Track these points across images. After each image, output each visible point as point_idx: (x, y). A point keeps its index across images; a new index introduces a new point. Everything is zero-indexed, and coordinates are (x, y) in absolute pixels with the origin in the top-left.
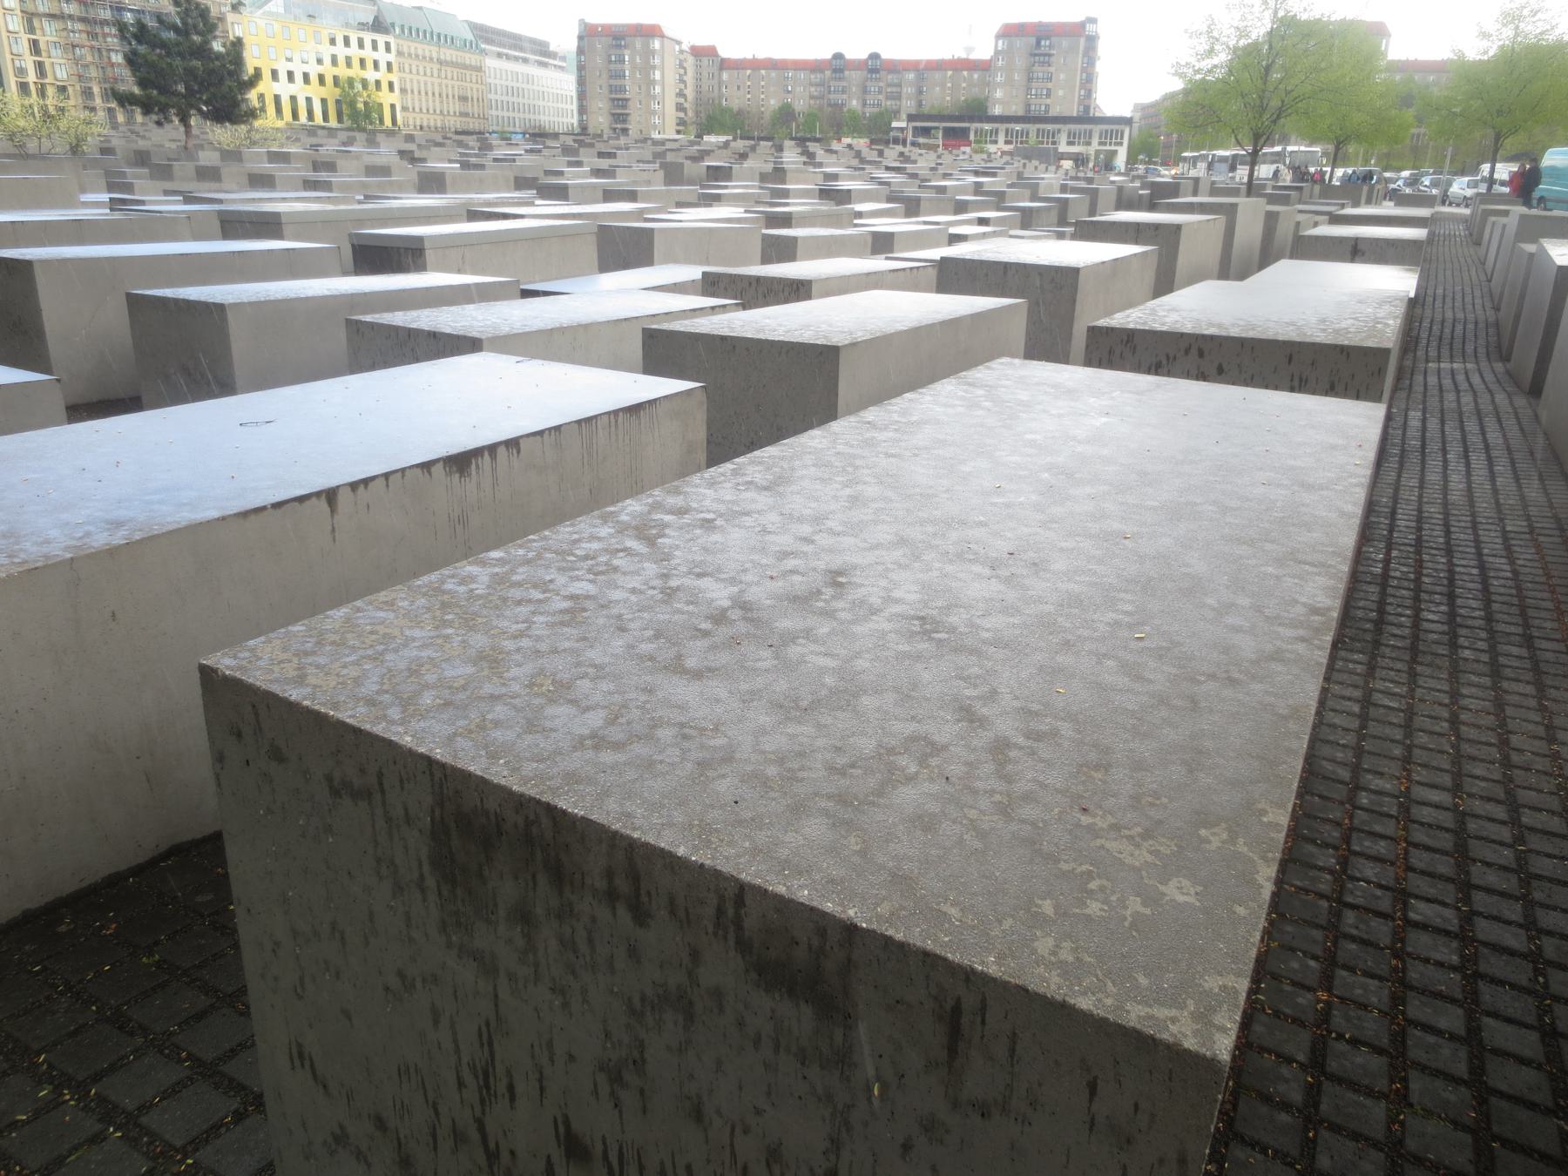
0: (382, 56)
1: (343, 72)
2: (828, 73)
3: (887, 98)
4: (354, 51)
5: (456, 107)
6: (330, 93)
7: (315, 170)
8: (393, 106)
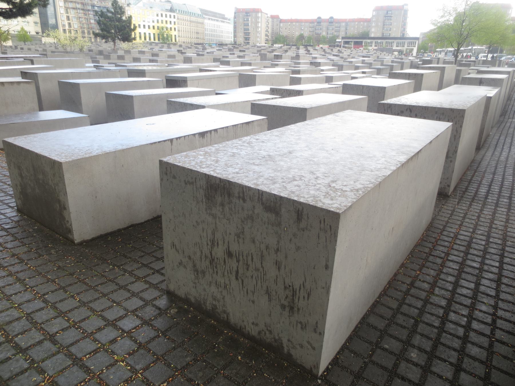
0: (173, 20)
1: (160, 25)
2: (316, 23)
3: (335, 32)
4: (164, 19)
5: (195, 35)
6: (156, 31)
7: (168, 58)
8: (175, 36)
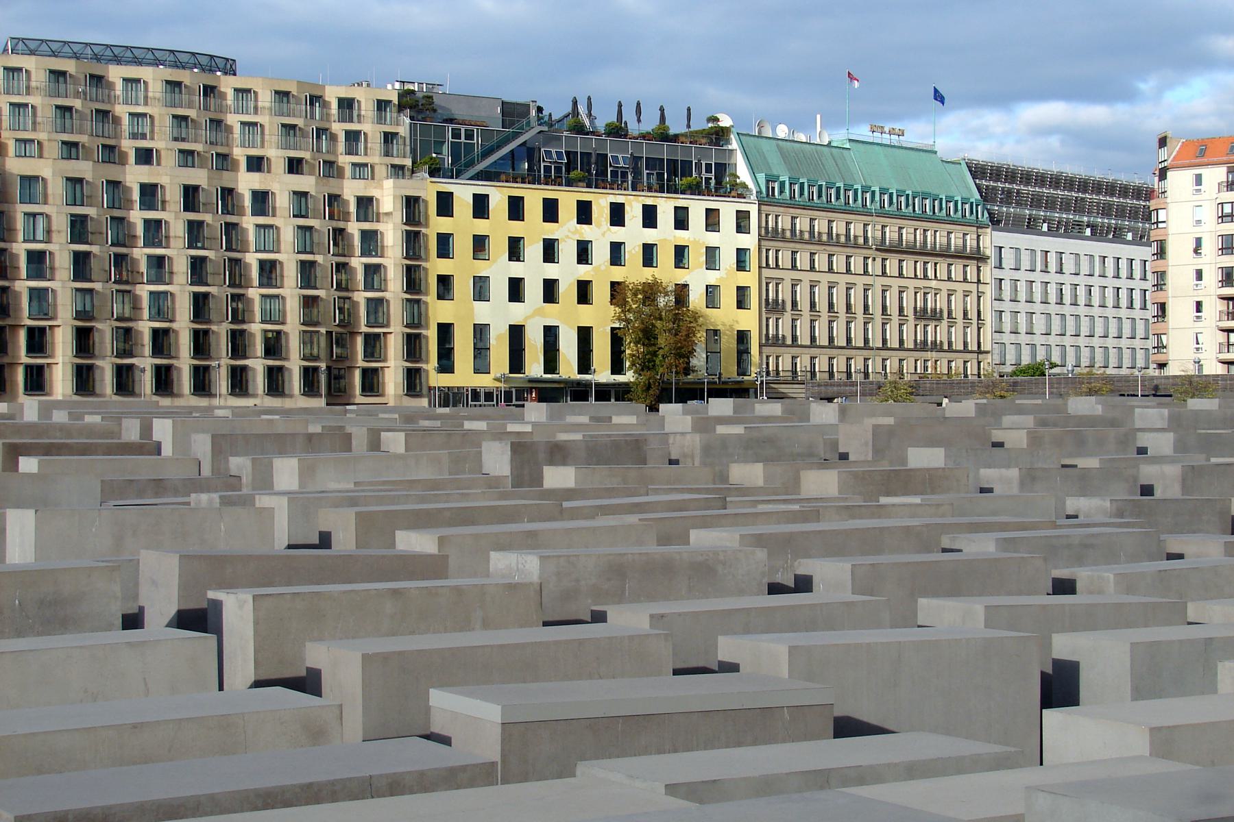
1: (633, 273)
6: (601, 317)
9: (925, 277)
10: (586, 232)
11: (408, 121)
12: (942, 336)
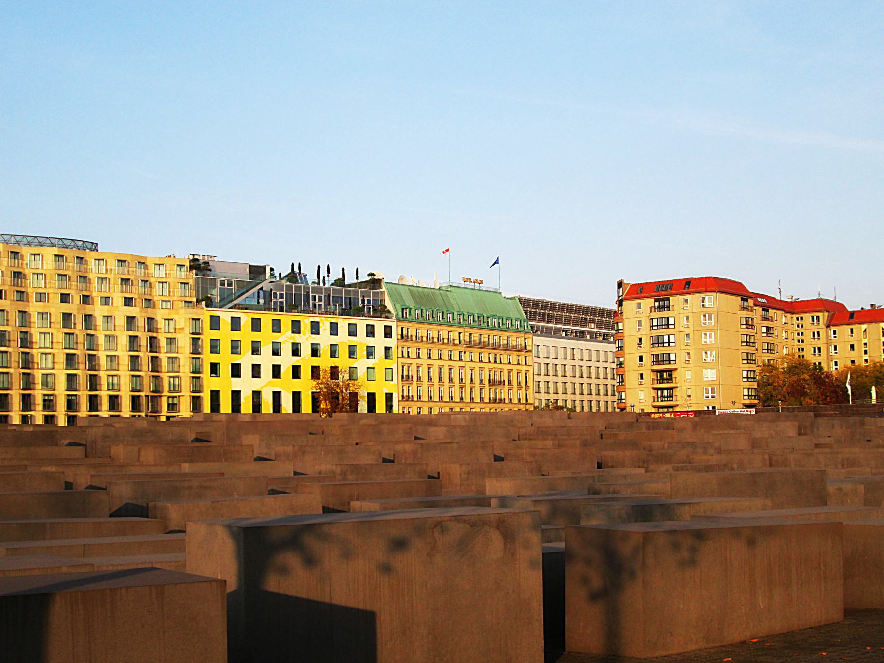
1: (325, 362)
6: (306, 386)
8: (389, 397)
9: (496, 362)
10: (297, 338)
11: (194, 276)
12: (505, 395)
